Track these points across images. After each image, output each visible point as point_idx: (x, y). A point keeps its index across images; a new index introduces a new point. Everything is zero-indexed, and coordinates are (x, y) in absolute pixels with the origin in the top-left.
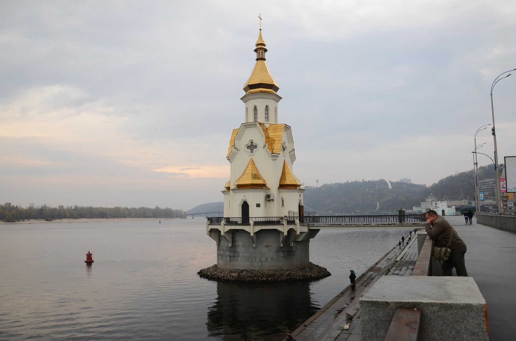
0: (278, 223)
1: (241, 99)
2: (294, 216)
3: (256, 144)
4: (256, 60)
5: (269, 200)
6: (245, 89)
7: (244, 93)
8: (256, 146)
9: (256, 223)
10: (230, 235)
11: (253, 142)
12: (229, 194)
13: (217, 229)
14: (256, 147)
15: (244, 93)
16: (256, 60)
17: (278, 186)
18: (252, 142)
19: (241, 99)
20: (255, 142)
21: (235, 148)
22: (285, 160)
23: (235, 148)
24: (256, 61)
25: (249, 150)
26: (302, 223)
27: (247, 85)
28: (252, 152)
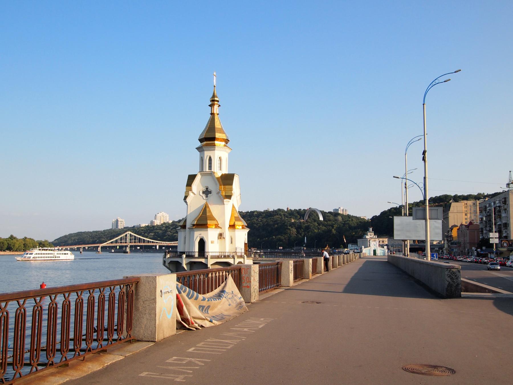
0: (228, 257)
1: (196, 148)
2: (242, 252)
3: (211, 190)
4: (210, 114)
5: (220, 238)
6: (201, 140)
7: (199, 144)
8: (211, 192)
9: (213, 257)
10: (189, 266)
11: (207, 188)
12: (186, 231)
13: (178, 262)
14: (210, 192)
15: (199, 144)
16: (210, 114)
17: (229, 226)
18: (207, 188)
19: (196, 148)
20: (210, 188)
21: (193, 192)
22: (234, 204)
23: (193, 192)
24: (210, 115)
25: (204, 196)
26: (248, 258)
27: (204, 137)
28: (207, 197)
